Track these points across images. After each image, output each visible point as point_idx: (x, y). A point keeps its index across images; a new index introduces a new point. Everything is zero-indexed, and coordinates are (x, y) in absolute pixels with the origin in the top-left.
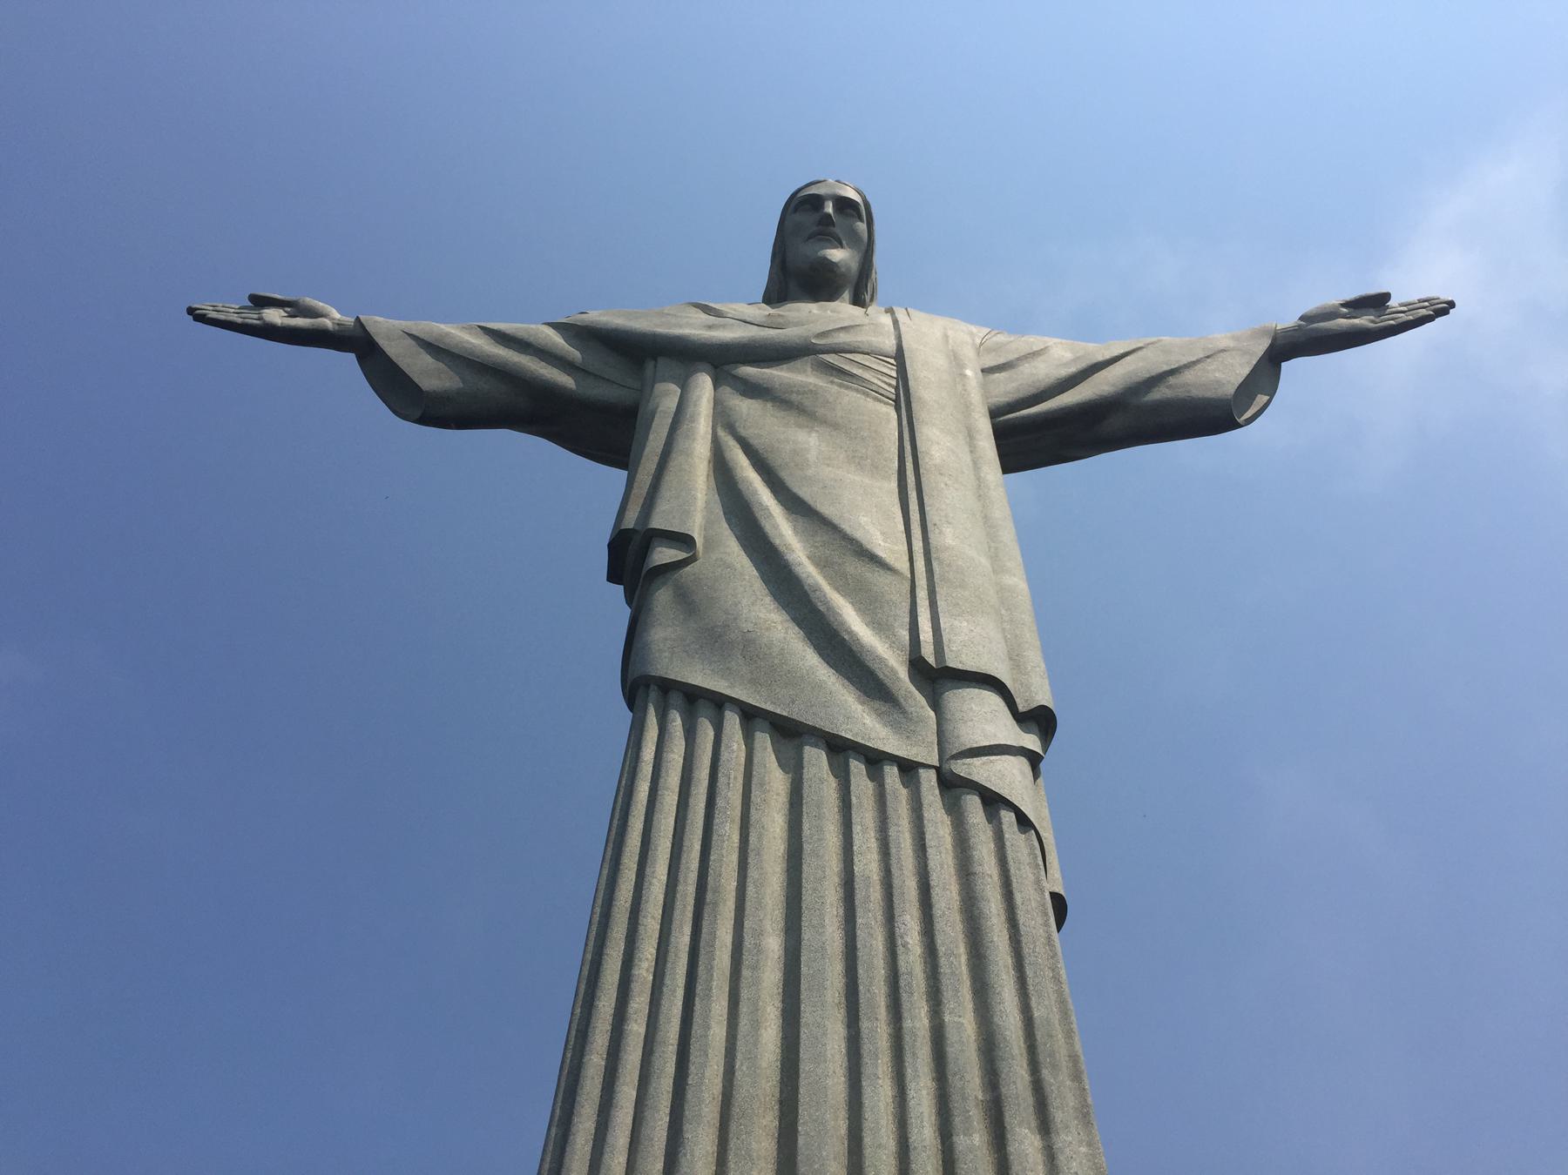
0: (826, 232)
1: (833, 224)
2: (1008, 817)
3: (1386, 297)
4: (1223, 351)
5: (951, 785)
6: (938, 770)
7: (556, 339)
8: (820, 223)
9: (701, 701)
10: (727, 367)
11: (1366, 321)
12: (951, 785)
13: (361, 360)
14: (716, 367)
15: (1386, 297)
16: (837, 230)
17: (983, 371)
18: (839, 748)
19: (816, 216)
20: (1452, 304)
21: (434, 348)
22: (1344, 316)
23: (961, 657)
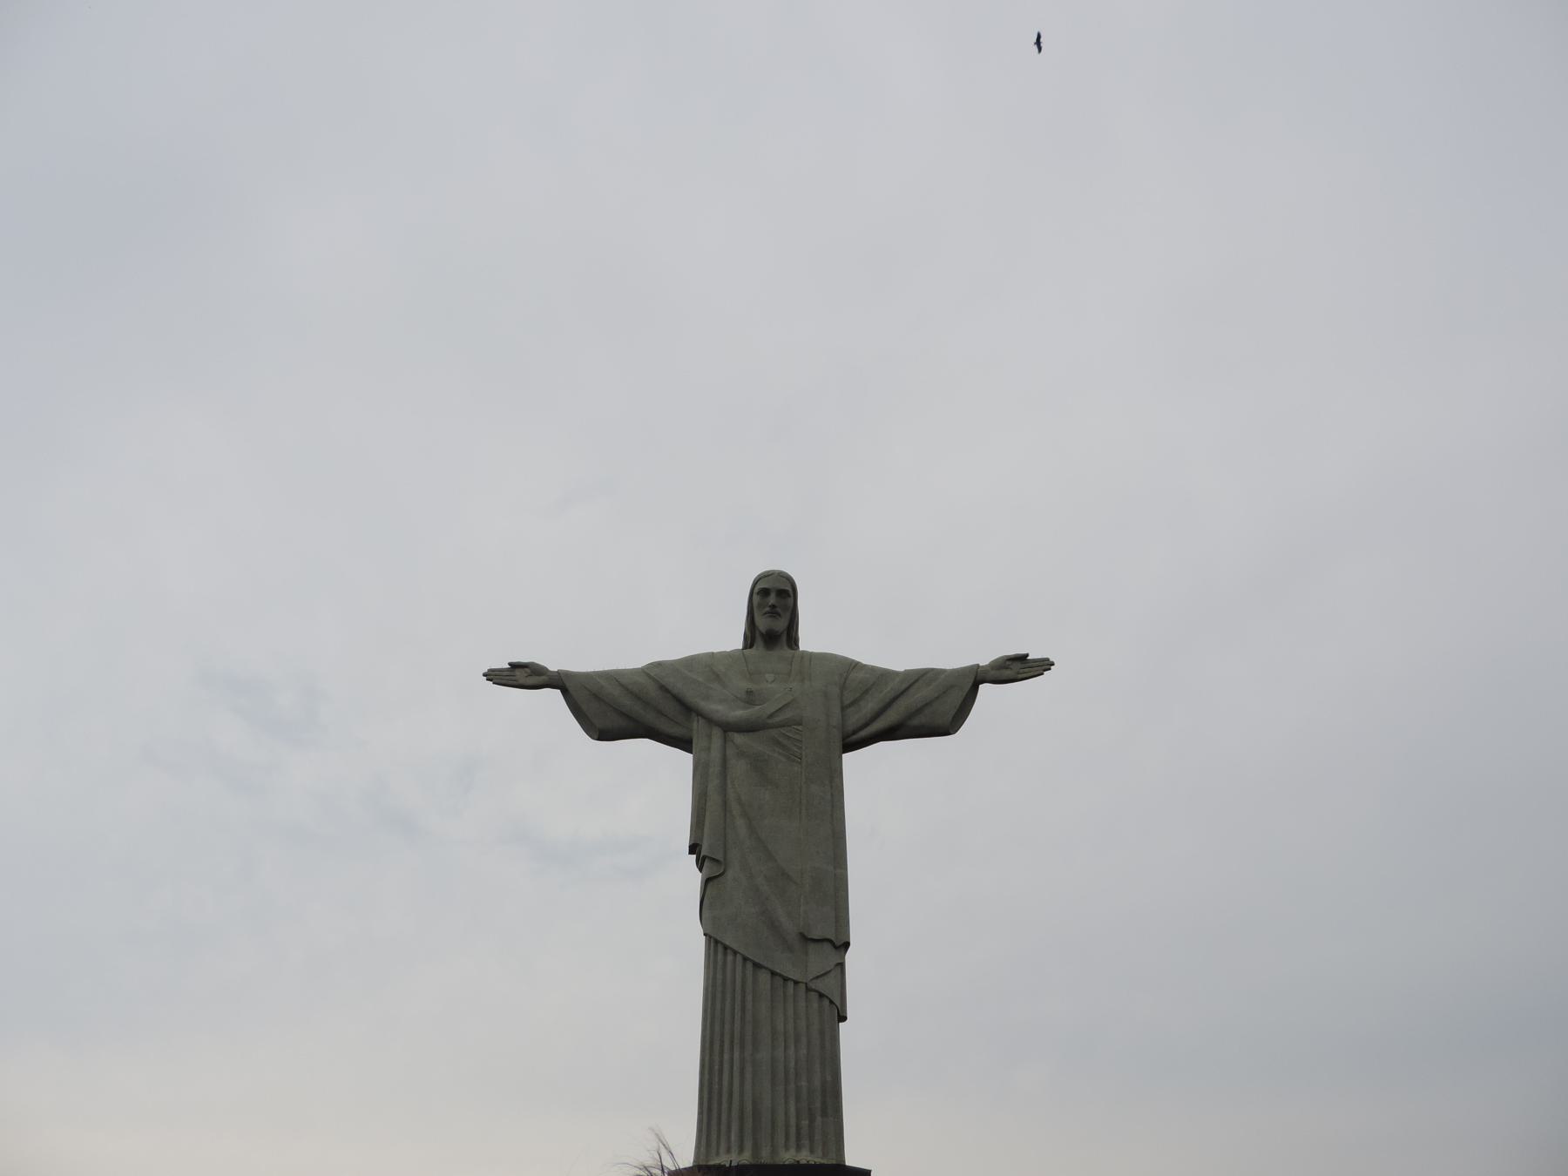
0: (773, 612)
2: (826, 1002)
4: (952, 686)
5: (808, 990)
11: (1017, 668)
12: (808, 990)
17: (843, 709)
18: (773, 974)
21: (597, 696)
22: (1007, 668)
23: (816, 934)
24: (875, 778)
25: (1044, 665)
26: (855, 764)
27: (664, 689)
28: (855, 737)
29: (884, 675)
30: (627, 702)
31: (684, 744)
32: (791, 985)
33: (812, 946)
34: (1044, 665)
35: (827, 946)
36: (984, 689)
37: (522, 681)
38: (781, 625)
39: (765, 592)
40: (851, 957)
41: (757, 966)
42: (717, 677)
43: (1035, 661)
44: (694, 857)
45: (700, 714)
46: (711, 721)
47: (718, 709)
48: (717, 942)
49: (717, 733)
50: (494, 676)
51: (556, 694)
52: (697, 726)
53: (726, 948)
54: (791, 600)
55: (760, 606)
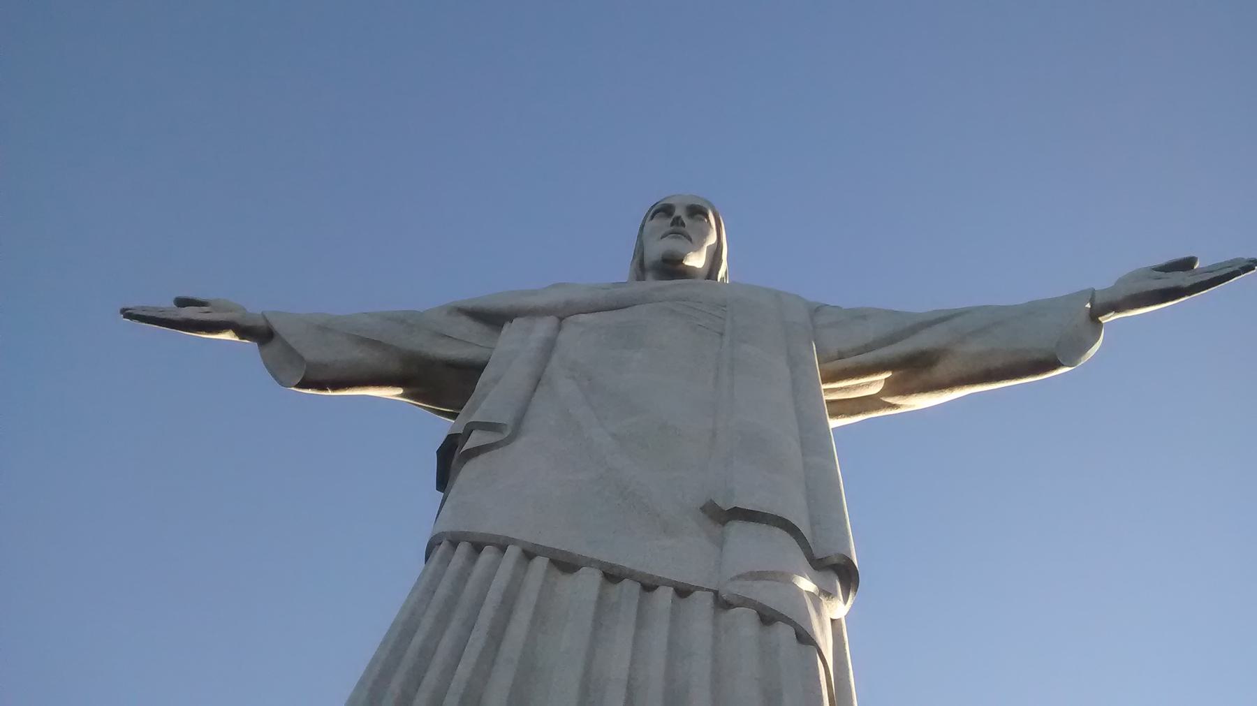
1: (683, 224)
2: (784, 633)
5: (722, 604)
6: (716, 593)
8: (672, 224)
12: (722, 604)
14: (561, 319)
16: (687, 230)
19: (670, 221)
32: (664, 596)
33: (736, 529)
41: (565, 564)
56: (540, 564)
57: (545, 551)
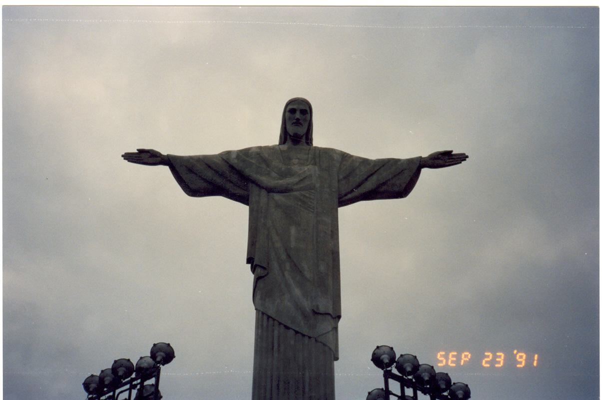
0: (297, 123)
3: (452, 151)
7: (225, 169)
9: (270, 319)
10: (271, 194)
11: (444, 159)
13: (170, 168)
15: (452, 151)
16: (301, 121)
20: (467, 157)
21: (190, 170)
24: (358, 222)
25: (462, 158)
26: (346, 213)
27: (232, 167)
28: (346, 198)
29: (365, 161)
30: (209, 174)
31: (243, 199)
33: (320, 317)
34: (462, 158)
35: (329, 317)
36: (425, 172)
37: (145, 161)
38: (302, 131)
39: (293, 111)
40: (341, 324)
41: (287, 328)
42: (264, 160)
43: (455, 155)
44: (249, 265)
45: (254, 182)
46: (260, 186)
47: (265, 180)
48: (263, 313)
49: (264, 192)
50: (129, 157)
51: (165, 170)
52: (254, 190)
53: (269, 317)
54: (308, 116)
55: (290, 119)
56: (282, 326)
57: (282, 324)
